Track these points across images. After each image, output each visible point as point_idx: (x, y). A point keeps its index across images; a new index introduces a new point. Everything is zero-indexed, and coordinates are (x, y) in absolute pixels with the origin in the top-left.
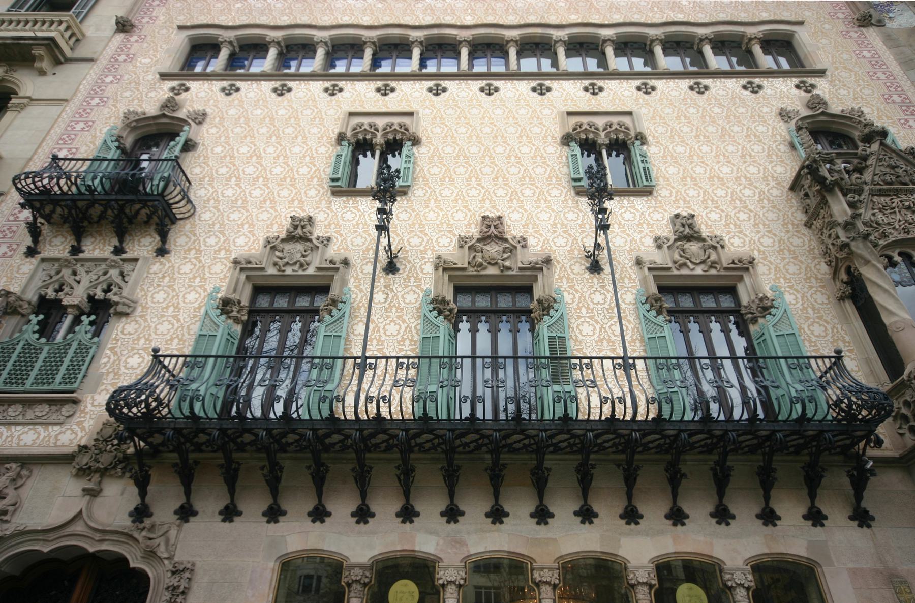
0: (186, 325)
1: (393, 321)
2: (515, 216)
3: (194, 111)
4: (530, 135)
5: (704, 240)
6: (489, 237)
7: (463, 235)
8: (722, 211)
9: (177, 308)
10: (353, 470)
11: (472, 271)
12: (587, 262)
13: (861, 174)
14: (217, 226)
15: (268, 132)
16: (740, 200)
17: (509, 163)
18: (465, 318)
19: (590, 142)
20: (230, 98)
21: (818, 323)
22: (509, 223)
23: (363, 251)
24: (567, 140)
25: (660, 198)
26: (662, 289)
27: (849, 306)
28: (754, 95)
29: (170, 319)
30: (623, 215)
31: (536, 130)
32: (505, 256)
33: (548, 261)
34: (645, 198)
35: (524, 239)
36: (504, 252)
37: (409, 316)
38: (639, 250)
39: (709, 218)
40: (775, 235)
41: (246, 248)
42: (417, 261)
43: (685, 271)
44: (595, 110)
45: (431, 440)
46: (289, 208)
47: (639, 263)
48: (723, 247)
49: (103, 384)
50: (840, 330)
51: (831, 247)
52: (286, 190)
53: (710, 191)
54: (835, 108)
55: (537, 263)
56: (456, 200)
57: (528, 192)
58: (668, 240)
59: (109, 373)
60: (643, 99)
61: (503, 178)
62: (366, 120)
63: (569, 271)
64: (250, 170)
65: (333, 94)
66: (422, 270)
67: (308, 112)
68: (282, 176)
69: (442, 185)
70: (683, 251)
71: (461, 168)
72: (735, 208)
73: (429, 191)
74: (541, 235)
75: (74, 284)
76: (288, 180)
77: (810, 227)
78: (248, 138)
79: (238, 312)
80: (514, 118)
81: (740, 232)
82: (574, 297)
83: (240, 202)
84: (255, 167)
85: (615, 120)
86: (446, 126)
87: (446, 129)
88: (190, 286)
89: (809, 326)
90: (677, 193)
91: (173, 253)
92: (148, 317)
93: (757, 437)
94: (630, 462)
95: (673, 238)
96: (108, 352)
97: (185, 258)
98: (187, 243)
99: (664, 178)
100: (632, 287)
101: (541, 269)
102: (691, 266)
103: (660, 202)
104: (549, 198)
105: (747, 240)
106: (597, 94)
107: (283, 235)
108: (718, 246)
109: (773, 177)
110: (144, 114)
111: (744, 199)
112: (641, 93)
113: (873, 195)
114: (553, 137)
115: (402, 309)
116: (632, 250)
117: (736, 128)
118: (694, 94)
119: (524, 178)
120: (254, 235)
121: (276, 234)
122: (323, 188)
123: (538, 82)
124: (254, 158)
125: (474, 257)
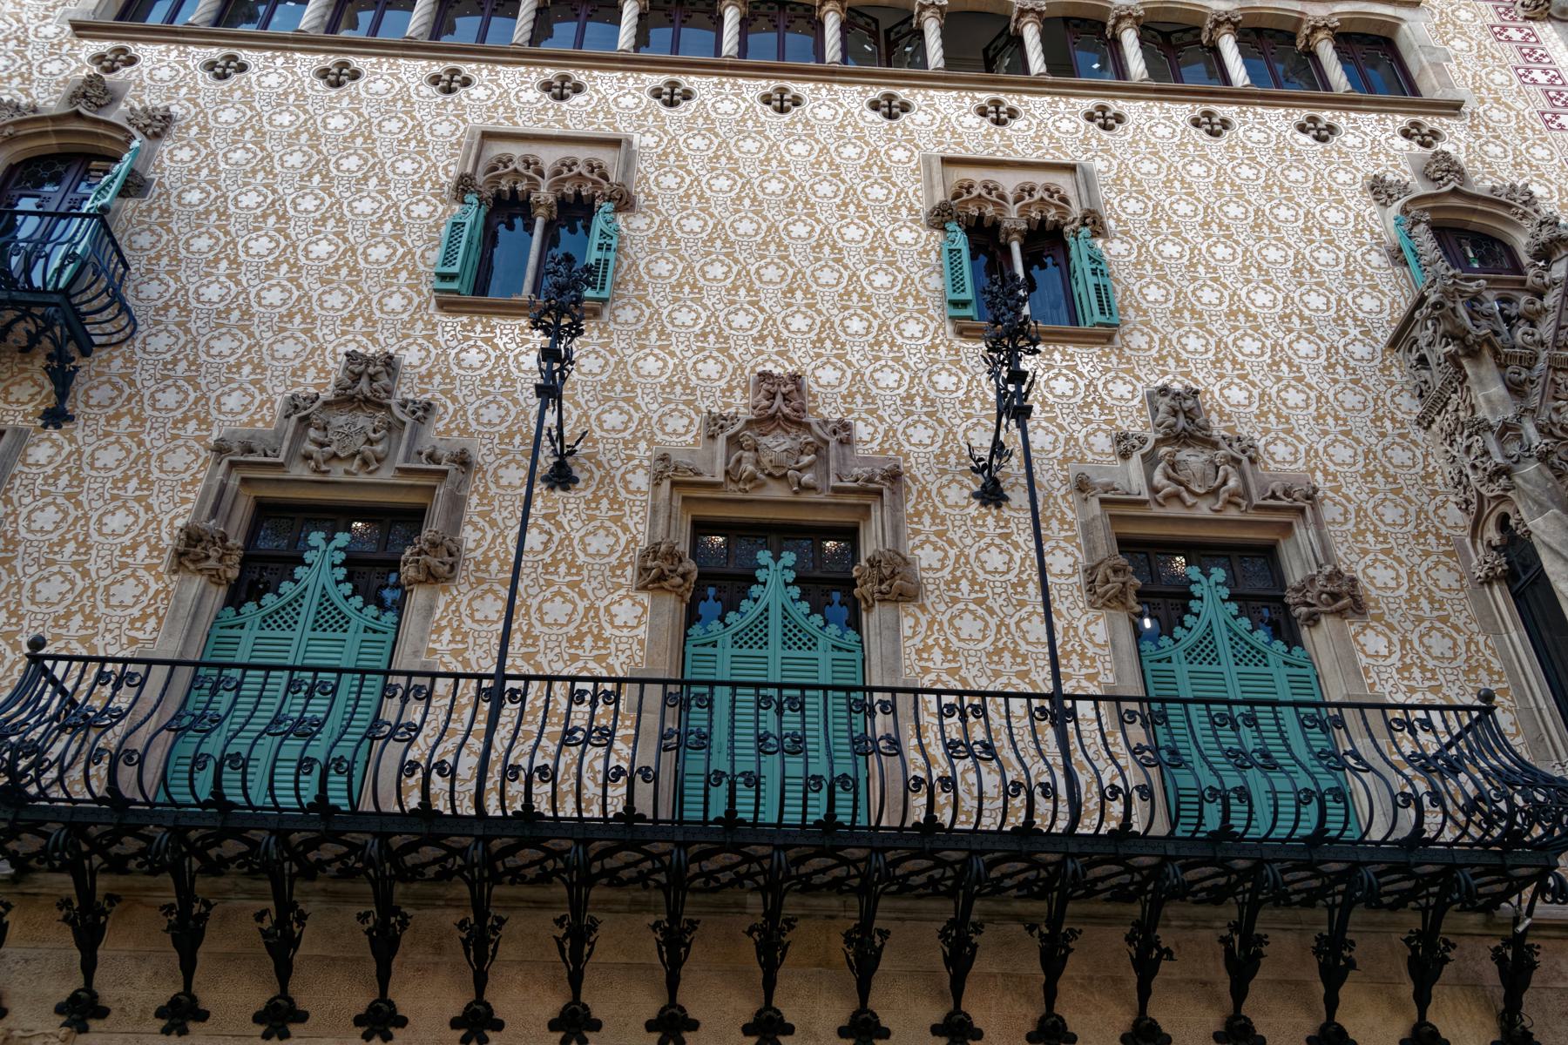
0: (102, 584)
1: (559, 593)
2: (828, 375)
3: (145, 110)
4: (865, 203)
5: (1215, 445)
6: (773, 417)
7: (715, 410)
8: (1253, 384)
9: (84, 545)
10: (461, 925)
11: (733, 492)
12: (975, 480)
13: (1533, 325)
14: (183, 365)
15: (304, 164)
16: (1290, 364)
17: (818, 260)
18: (711, 591)
19: (987, 224)
20: (225, 85)
21: (1439, 630)
22: (815, 389)
23: (502, 437)
24: (940, 217)
25: (1127, 352)
26: (1126, 545)
27: (1499, 597)
28: (1319, 146)
29: (67, 569)
30: (1052, 383)
31: (877, 192)
32: (806, 459)
33: (895, 476)
34: (1097, 350)
35: (846, 427)
36: (802, 452)
37: (594, 584)
38: (1082, 461)
39: (1226, 399)
40: (1358, 441)
41: (244, 418)
42: (617, 463)
43: (1174, 510)
44: (999, 156)
45: (636, 864)
46: (344, 333)
47: (1082, 486)
48: (1252, 461)
50: (1482, 646)
51: (1469, 471)
52: (337, 293)
53: (1230, 341)
54: (1482, 183)
55: (870, 480)
56: (704, 335)
57: (856, 325)
58: (1144, 441)
60: (1099, 140)
61: (806, 292)
62: (517, 151)
63: (937, 500)
64: (261, 245)
65: (449, 90)
66: (626, 484)
67: (393, 125)
68: (330, 263)
69: (676, 300)
70: (1173, 466)
71: (717, 264)
72: (1279, 379)
73: (647, 314)
74: (881, 420)
76: (344, 271)
77: (1427, 428)
78: (260, 175)
79: (220, 560)
80: (831, 163)
81: (1289, 432)
82: (946, 556)
83: (236, 315)
84: (271, 239)
85: (1040, 179)
86: (689, 173)
87: (688, 180)
88: (114, 498)
89: (1421, 637)
90: (1162, 341)
92: (18, 564)
93: (1318, 875)
94: (1055, 920)
95: (1152, 436)
97: (107, 434)
99: (1138, 309)
100: (1066, 539)
101: (880, 493)
102: (1190, 500)
103: (1129, 361)
104: (899, 340)
105: (1302, 448)
106: (1004, 123)
107: (327, 394)
108: (1244, 459)
109: (1355, 319)
110: (35, 110)
111: (1296, 361)
112: (1093, 126)
113: (1556, 370)
114: (910, 209)
115: (580, 568)
116: (1066, 460)
117: (1283, 213)
118: (1200, 135)
119: (848, 294)
120: (262, 390)
121: (312, 390)
122: (420, 293)
123: (884, 90)
124: (272, 220)
125: (739, 461)
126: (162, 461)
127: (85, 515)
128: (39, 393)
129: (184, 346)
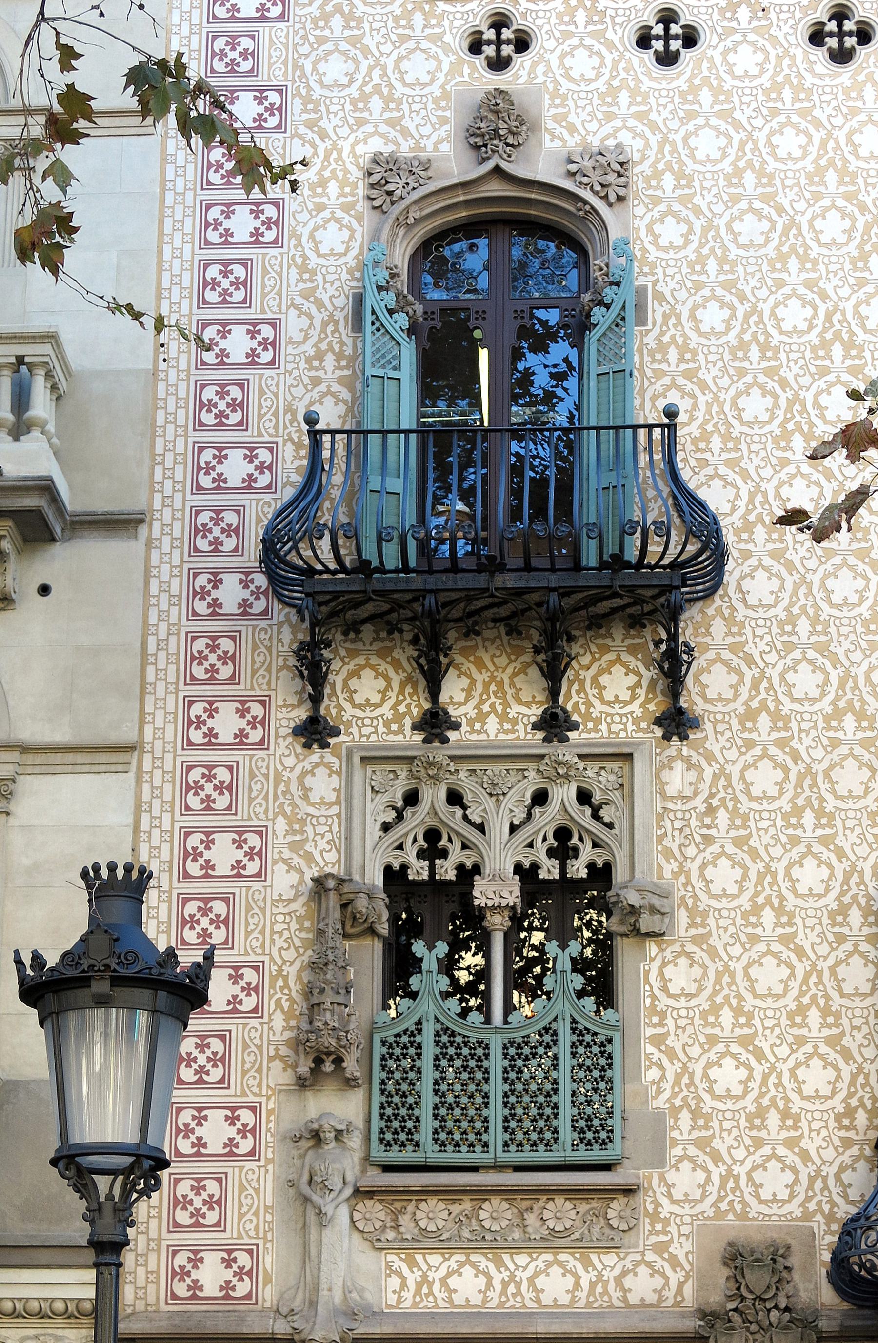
15: (849, 232)
49: (674, 1143)
59: (675, 1111)
75: (473, 835)
78: (793, 264)
88: (795, 841)
91: (708, 726)
96: (650, 1049)
97: (750, 744)
98: (735, 688)
126: (833, 783)
127: (768, 867)
128: (638, 684)
129: (795, 592)
